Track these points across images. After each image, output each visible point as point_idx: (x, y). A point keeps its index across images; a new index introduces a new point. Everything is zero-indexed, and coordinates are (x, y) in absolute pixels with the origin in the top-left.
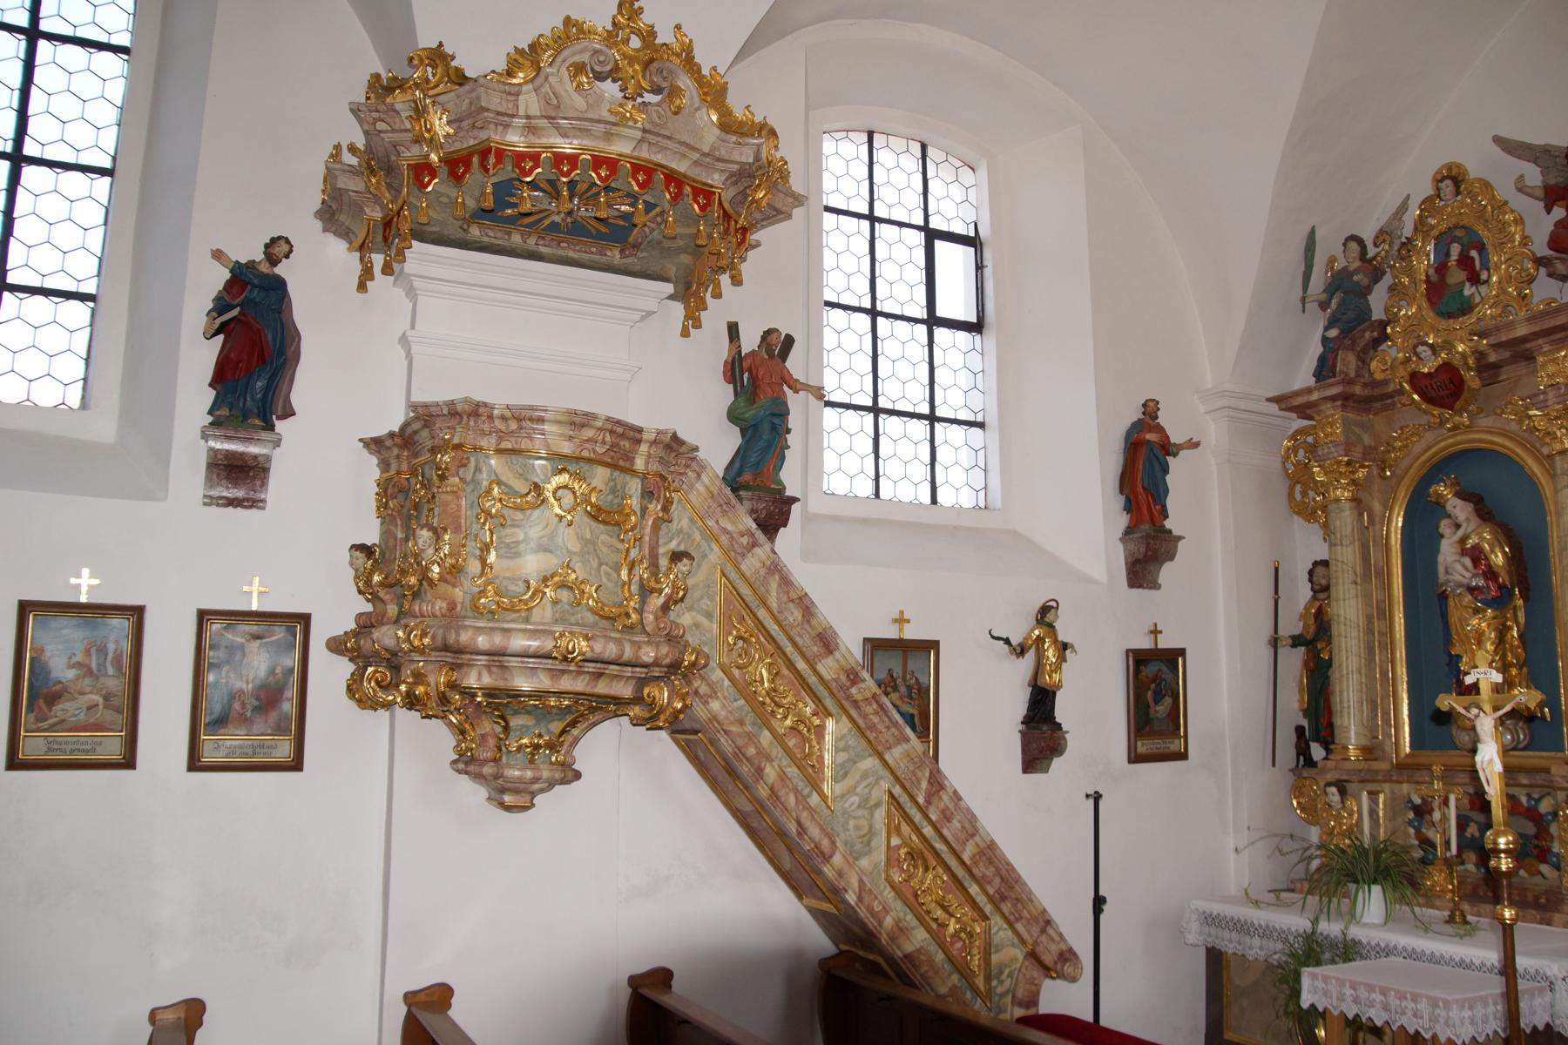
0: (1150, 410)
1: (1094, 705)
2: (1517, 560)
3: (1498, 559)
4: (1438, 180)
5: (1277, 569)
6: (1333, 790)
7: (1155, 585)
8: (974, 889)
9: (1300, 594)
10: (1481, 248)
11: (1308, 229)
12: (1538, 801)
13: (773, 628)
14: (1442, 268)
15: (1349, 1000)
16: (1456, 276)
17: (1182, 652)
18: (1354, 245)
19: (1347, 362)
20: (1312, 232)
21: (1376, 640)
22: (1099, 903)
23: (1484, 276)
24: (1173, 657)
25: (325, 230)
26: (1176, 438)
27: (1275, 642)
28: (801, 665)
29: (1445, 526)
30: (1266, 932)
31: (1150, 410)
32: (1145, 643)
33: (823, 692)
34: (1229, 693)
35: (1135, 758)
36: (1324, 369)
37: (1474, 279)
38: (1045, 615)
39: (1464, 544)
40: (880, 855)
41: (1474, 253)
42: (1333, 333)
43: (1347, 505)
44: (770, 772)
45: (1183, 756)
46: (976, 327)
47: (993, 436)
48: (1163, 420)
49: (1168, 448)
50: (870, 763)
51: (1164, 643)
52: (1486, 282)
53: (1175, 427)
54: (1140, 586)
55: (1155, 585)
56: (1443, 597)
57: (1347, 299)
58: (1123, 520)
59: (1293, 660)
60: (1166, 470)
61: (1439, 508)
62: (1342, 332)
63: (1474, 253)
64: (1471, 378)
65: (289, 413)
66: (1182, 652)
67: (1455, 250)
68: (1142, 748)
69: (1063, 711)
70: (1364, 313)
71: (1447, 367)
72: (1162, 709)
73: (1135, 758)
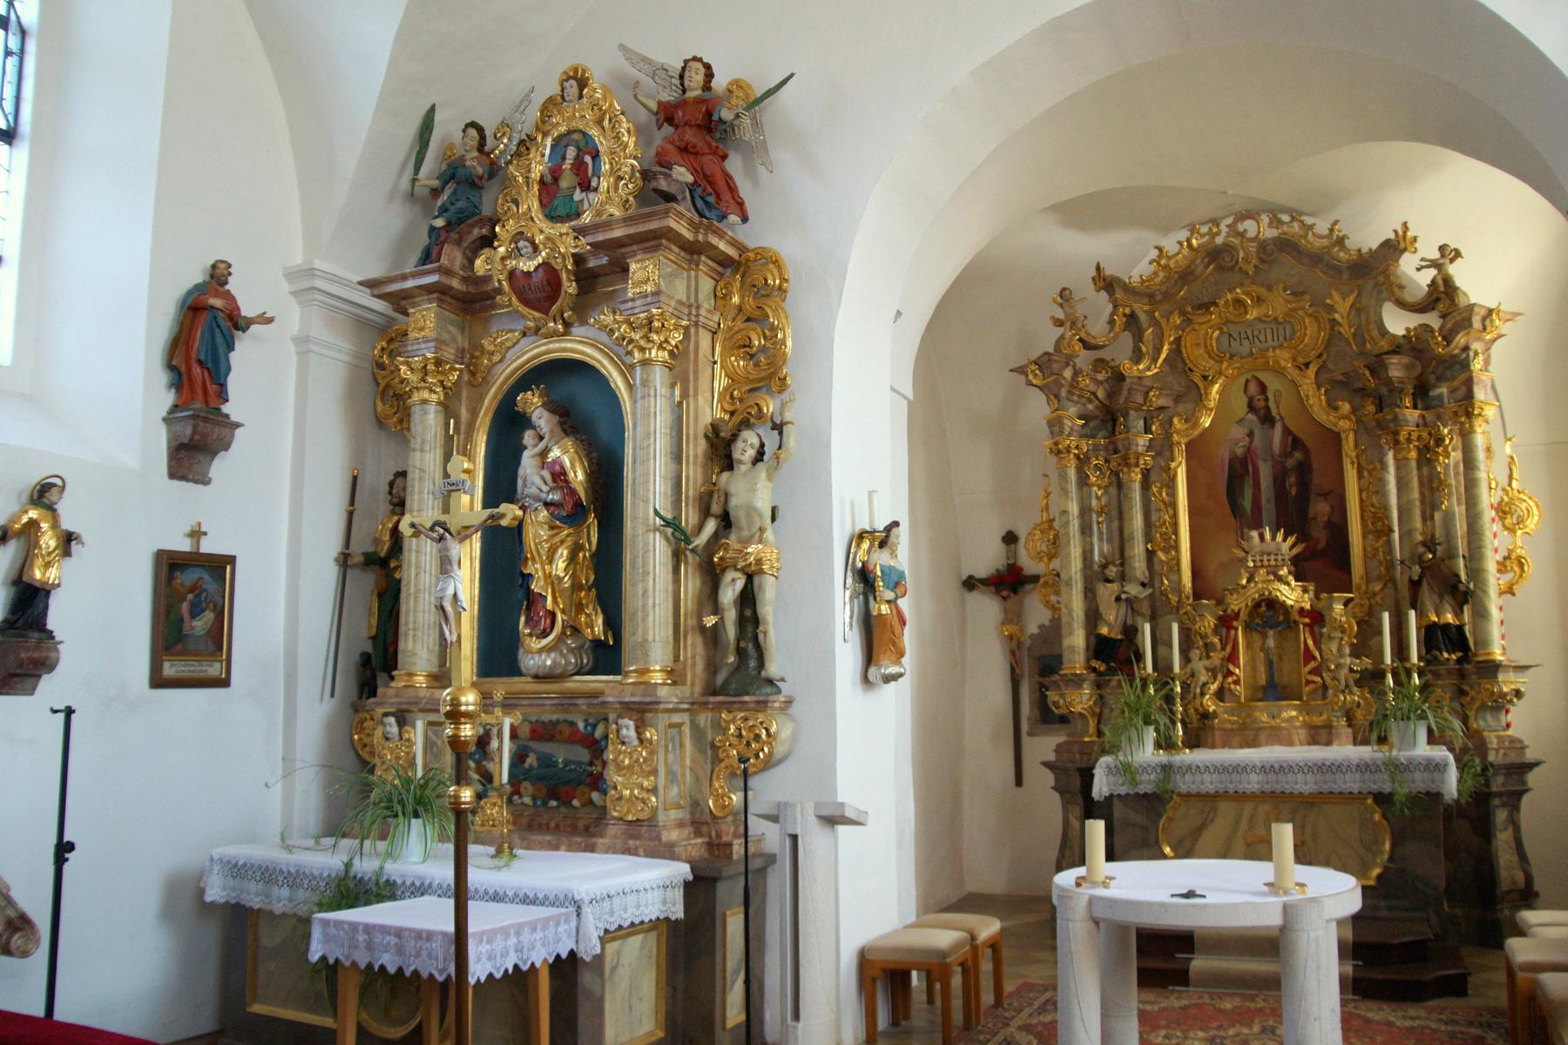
0: (218, 275)
2: (592, 476)
3: (578, 476)
5: (355, 479)
6: (392, 720)
7: (205, 481)
10: (596, 156)
11: (428, 106)
12: (594, 726)
14: (556, 173)
15: (362, 946)
17: (232, 560)
18: (473, 132)
20: (432, 109)
22: (63, 849)
23: (594, 184)
24: (220, 566)
26: (247, 310)
27: (344, 560)
29: (528, 437)
31: (218, 275)
32: (184, 545)
34: (285, 609)
35: (158, 681)
37: (586, 186)
38: (43, 495)
41: (588, 159)
43: (432, 408)
45: (224, 683)
48: (233, 286)
49: (236, 322)
51: (207, 547)
52: (596, 190)
53: (247, 294)
54: (183, 478)
55: (205, 481)
57: (458, 193)
58: (168, 399)
59: (364, 583)
60: (230, 347)
62: (449, 224)
63: (588, 159)
64: (570, 287)
66: (232, 560)
67: (571, 152)
68: (169, 670)
70: (476, 209)
71: (545, 265)
72: (201, 624)
73: (158, 681)
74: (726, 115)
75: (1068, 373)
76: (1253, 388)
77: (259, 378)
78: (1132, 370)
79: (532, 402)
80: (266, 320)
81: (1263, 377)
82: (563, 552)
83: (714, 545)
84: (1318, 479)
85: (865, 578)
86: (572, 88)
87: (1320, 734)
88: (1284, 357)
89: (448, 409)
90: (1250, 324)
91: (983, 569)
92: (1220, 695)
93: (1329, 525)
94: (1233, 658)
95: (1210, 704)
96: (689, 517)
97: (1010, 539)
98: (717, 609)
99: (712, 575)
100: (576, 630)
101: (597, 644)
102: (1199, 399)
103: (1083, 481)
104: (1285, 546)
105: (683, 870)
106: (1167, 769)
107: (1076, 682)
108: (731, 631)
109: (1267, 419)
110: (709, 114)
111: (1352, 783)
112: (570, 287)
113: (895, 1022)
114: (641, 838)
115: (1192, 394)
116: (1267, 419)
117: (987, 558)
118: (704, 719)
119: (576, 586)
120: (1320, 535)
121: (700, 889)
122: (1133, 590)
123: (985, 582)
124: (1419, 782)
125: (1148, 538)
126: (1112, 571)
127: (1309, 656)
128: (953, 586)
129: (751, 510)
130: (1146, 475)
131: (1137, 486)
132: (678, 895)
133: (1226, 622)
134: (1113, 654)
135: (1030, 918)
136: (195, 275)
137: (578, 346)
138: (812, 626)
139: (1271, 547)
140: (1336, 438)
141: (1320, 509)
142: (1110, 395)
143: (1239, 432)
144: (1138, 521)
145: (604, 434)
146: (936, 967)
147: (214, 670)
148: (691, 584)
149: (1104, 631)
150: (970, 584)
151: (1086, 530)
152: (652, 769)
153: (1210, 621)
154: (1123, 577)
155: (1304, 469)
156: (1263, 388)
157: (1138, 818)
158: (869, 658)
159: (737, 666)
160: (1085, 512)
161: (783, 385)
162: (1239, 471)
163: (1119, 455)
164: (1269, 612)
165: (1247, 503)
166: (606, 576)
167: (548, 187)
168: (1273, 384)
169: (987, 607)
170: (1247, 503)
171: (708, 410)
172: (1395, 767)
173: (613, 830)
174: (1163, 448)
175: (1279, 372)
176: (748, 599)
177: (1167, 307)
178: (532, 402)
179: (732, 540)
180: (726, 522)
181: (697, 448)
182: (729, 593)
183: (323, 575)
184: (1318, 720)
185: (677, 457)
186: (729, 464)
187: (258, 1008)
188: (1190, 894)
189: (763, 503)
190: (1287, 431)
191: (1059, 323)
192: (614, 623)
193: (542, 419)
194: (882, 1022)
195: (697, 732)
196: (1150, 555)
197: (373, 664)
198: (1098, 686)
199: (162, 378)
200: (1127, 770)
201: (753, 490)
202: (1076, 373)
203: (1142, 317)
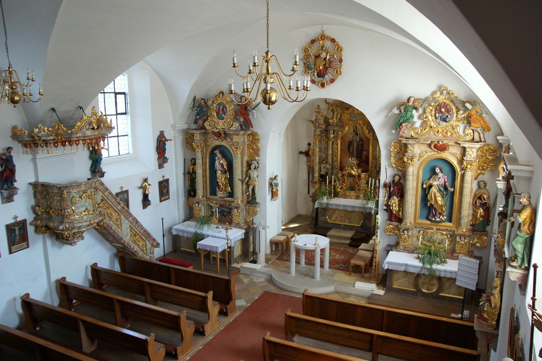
1: (154, 193)
4: (220, 93)
8: (143, 237)
9: (189, 163)
10: (226, 108)
13: (110, 203)
16: (221, 112)
17: (168, 179)
19: (200, 122)
21: (204, 176)
25: (11, 137)
26: (167, 138)
27: (184, 174)
28: (115, 208)
29: (217, 158)
30: (188, 232)
31: (162, 133)
32: (161, 179)
33: (118, 212)
34: (177, 186)
35: (161, 201)
36: (196, 122)
37: (225, 114)
38: (146, 180)
39: (220, 162)
40: (129, 236)
42: (198, 117)
44: (113, 228)
45: (169, 198)
46: (125, 113)
47: (129, 138)
48: (165, 134)
50: (127, 221)
56: (216, 171)
58: (157, 156)
60: (165, 144)
61: (216, 155)
65: (16, 181)
67: (221, 107)
68: (162, 199)
69: (150, 198)
71: (219, 132)
74: (249, 108)
75: (317, 124)
76: (355, 127)
77: (169, 146)
78: (331, 121)
79: (217, 152)
80: (171, 140)
81: (357, 125)
82: (223, 179)
83: (248, 181)
84: (365, 147)
85: (271, 185)
86: (221, 95)
87: (357, 197)
88: (361, 122)
89: (202, 151)
90: (355, 114)
91: (303, 150)
92: (341, 188)
93: (366, 156)
94: (344, 182)
95: (339, 190)
96: (244, 176)
97: (309, 144)
98: (248, 192)
99: (248, 186)
100: (226, 190)
101: (229, 192)
102: (344, 129)
103: (320, 142)
104: (355, 162)
105: (244, 231)
106: (328, 204)
107: (316, 183)
108: (251, 194)
109: (357, 134)
110: (246, 107)
111: (357, 210)
112: (223, 135)
113: (276, 249)
114: (238, 226)
115: (343, 127)
116: (357, 134)
117: (304, 148)
118: (247, 207)
119: (226, 183)
120: (364, 158)
121: (247, 234)
122: (328, 166)
123: (303, 153)
124: (368, 211)
125: (332, 155)
126: (324, 162)
127: (357, 183)
128: (298, 153)
129: (254, 177)
130: (333, 143)
131: (331, 145)
132: (244, 235)
133: (343, 175)
134: (323, 177)
135: (307, 223)
136: (159, 134)
137: (224, 143)
138: (263, 193)
139: (352, 162)
140: (369, 139)
141: (365, 153)
142: (326, 127)
143: (351, 136)
144: (330, 152)
145: (229, 157)
146: (281, 243)
147: (167, 197)
148: (245, 187)
149: (322, 173)
150: (301, 153)
151: (320, 151)
152: (238, 216)
153: (340, 175)
154: (327, 163)
155: (362, 145)
156: (356, 128)
157: (323, 212)
158: (272, 197)
159: (252, 201)
160: (320, 148)
161: (259, 156)
162: (350, 144)
163: (328, 138)
164: (350, 175)
165: (351, 150)
166: (231, 181)
167: (218, 113)
168: (358, 127)
169: (304, 158)
170: (351, 150)
171: (246, 158)
172: (364, 208)
173: (234, 224)
174: (336, 138)
175: (360, 125)
176: (253, 190)
177: (340, 108)
178: (217, 152)
179: (251, 181)
180: (250, 177)
181: (245, 165)
182: (250, 189)
183: (181, 177)
184: (357, 194)
185: (242, 166)
186: (250, 169)
187: (182, 249)
188: (305, 245)
189: (255, 176)
190: (360, 137)
191: (316, 112)
192: (232, 189)
193: (219, 155)
194: (274, 249)
195: (246, 209)
196: (332, 158)
197: (191, 192)
198: (320, 184)
199: (156, 153)
200: (320, 204)
201: (254, 174)
202: (319, 124)
203: (335, 109)
